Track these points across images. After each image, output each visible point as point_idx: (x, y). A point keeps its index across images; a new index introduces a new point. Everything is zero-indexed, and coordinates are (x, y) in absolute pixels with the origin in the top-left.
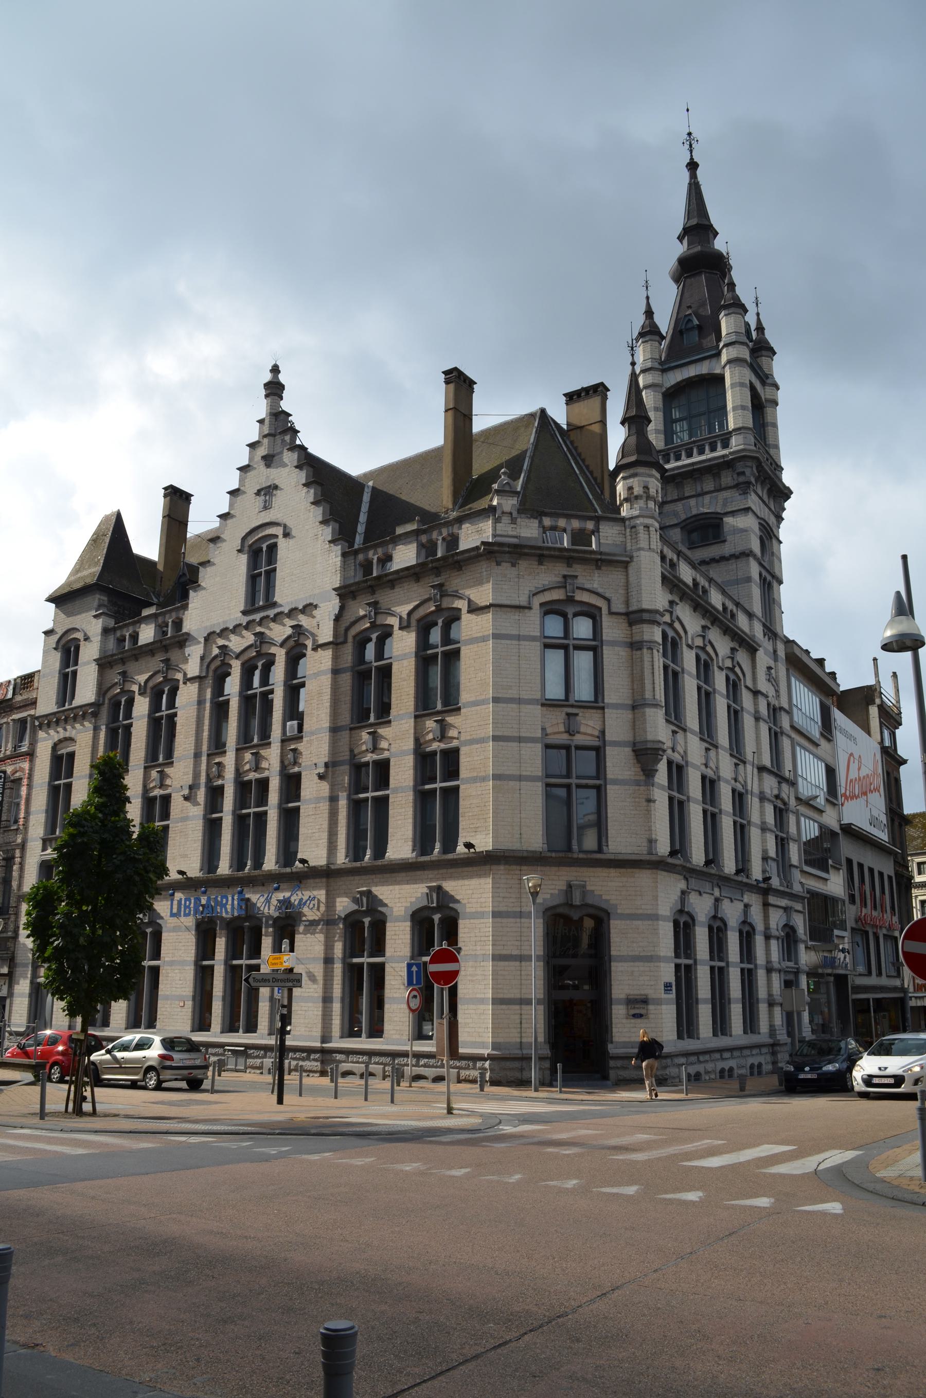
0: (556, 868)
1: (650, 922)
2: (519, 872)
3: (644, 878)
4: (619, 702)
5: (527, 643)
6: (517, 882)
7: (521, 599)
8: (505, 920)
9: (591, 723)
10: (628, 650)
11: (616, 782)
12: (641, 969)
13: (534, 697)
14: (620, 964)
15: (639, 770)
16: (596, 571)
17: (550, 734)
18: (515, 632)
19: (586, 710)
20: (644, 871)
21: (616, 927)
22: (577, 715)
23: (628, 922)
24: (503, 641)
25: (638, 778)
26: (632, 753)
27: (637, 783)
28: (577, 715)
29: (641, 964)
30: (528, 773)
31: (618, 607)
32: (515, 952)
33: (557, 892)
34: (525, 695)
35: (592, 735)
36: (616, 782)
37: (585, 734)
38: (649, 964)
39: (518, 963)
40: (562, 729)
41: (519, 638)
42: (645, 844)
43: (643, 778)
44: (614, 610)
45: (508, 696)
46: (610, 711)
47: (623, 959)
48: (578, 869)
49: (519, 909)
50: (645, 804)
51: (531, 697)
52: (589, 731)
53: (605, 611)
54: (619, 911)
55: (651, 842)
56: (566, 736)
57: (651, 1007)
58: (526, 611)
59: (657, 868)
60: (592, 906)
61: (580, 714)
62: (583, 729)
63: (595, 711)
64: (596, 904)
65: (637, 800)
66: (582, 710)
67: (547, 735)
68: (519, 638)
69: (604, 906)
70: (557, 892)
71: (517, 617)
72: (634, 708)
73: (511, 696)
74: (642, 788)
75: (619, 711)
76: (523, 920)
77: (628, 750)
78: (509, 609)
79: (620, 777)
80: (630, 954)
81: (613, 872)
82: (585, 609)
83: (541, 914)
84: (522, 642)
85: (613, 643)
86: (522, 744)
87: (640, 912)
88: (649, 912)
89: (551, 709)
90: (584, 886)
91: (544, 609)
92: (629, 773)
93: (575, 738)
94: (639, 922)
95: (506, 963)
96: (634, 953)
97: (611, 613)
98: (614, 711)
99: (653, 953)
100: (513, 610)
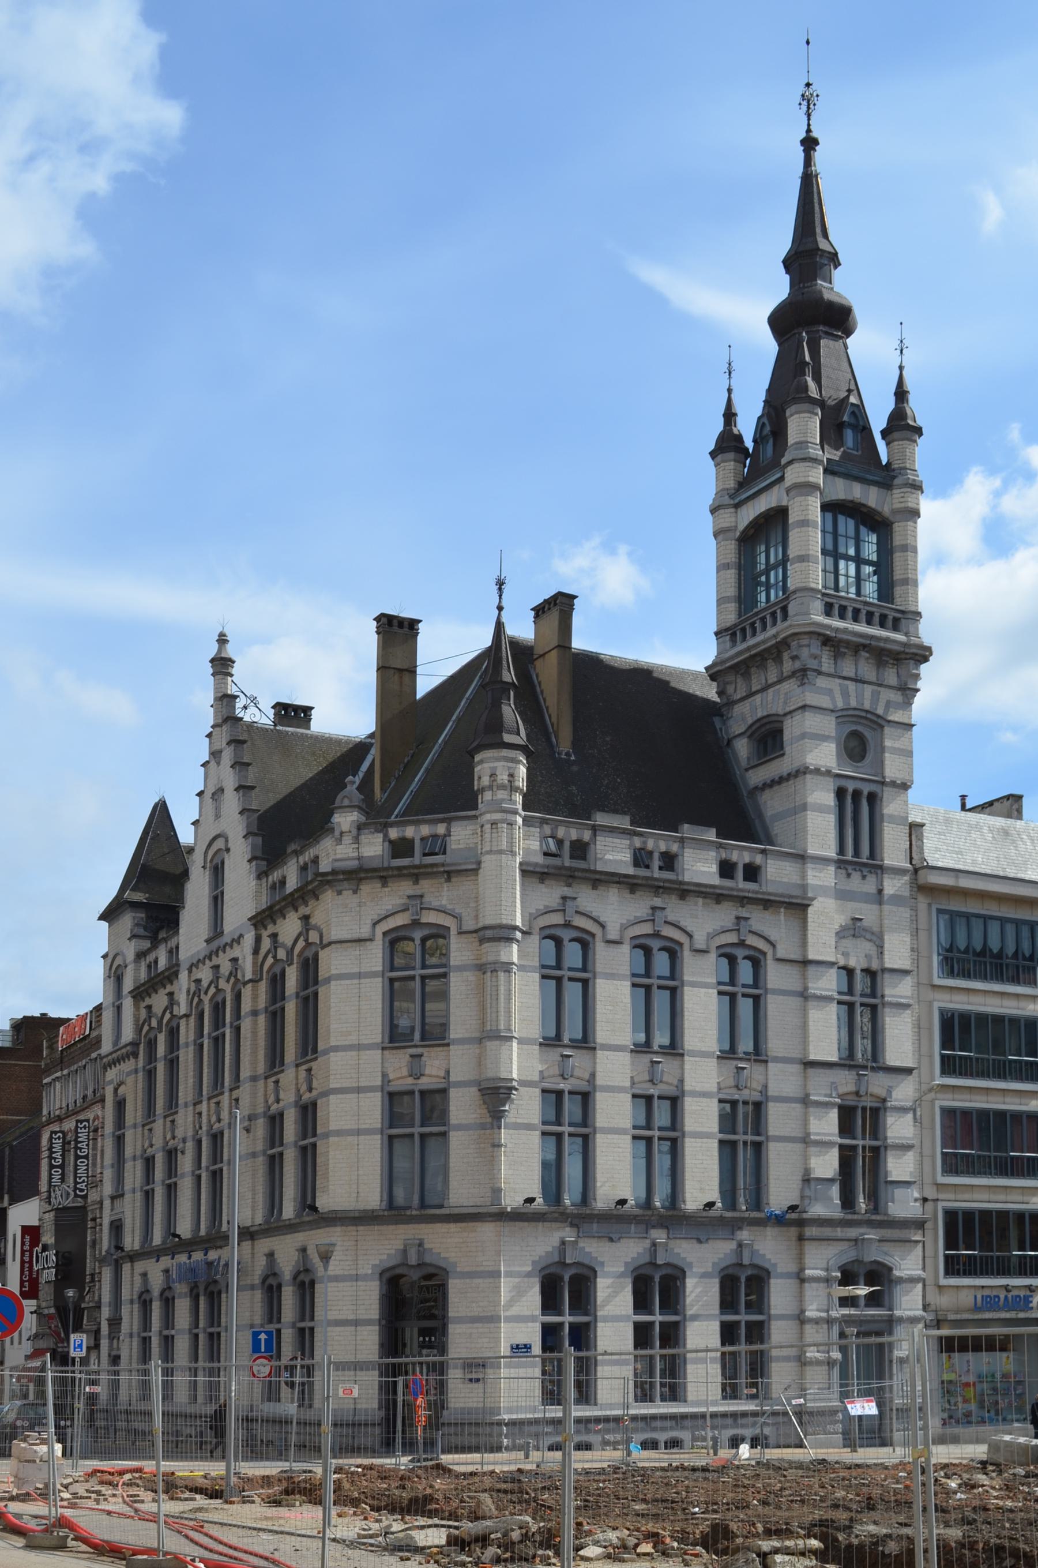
0: (393, 1227)
1: (491, 1280)
2: (354, 1233)
3: (487, 1230)
4: (467, 1035)
5: (368, 980)
6: (354, 1243)
7: (362, 931)
8: (341, 1284)
9: (436, 1062)
10: (477, 973)
11: (460, 1127)
12: (481, 1330)
13: (375, 1041)
14: (458, 1326)
15: (486, 1111)
16: (445, 885)
17: (393, 1080)
18: (356, 970)
19: (431, 1049)
20: (487, 1224)
21: (455, 1287)
22: (421, 1056)
23: (468, 1280)
24: (343, 982)
25: (483, 1121)
26: (478, 1093)
27: (483, 1127)
28: (421, 1056)
29: (480, 1325)
30: (367, 1126)
31: (469, 924)
32: (352, 1317)
33: (393, 1252)
34: (365, 1041)
35: (438, 1077)
36: (460, 1127)
37: (430, 1076)
38: (489, 1325)
39: (353, 1328)
40: (405, 1072)
41: (360, 976)
42: (489, 1194)
43: (489, 1120)
44: (465, 928)
45: (347, 1043)
46: (456, 1047)
47: (461, 1320)
48: (416, 1226)
49: (355, 1272)
50: (491, 1149)
51: (371, 1041)
52: (434, 1072)
53: (453, 931)
54: (458, 1269)
55: (497, 1192)
56: (410, 1081)
57: (489, 1371)
58: (368, 943)
59: (500, 1220)
60: (431, 1265)
61: (425, 1054)
62: (427, 1072)
63: (441, 1049)
64: (434, 1262)
65: (482, 1145)
66: (427, 1049)
67: (389, 1081)
68: (360, 976)
69: (443, 1265)
70: (393, 1252)
71: (358, 953)
72: (480, 1041)
73: (350, 1043)
74: (488, 1132)
75: (466, 1046)
76: (359, 1283)
77: (474, 1090)
78: (349, 944)
79: (464, 1122)
80: (469, 1314)
81: (453, 1227)
82: (434, 931)
83: (377, 1276)
84: (363, 981)
85: (461, 968)
86: (361, 1095)
87: (482, 1269)
88: (490, 1269)
89: (394, 1051)
90: (421, 1245)
91: (387, 939)
92: (474, 1116)
93: (420, 1081)
94: (480, 1281)
95: (342, 1328)
96: (472, 1314)
97: (460, 933)
98: (461, 1047)
99: (493, 1313)
100: (354, 944)
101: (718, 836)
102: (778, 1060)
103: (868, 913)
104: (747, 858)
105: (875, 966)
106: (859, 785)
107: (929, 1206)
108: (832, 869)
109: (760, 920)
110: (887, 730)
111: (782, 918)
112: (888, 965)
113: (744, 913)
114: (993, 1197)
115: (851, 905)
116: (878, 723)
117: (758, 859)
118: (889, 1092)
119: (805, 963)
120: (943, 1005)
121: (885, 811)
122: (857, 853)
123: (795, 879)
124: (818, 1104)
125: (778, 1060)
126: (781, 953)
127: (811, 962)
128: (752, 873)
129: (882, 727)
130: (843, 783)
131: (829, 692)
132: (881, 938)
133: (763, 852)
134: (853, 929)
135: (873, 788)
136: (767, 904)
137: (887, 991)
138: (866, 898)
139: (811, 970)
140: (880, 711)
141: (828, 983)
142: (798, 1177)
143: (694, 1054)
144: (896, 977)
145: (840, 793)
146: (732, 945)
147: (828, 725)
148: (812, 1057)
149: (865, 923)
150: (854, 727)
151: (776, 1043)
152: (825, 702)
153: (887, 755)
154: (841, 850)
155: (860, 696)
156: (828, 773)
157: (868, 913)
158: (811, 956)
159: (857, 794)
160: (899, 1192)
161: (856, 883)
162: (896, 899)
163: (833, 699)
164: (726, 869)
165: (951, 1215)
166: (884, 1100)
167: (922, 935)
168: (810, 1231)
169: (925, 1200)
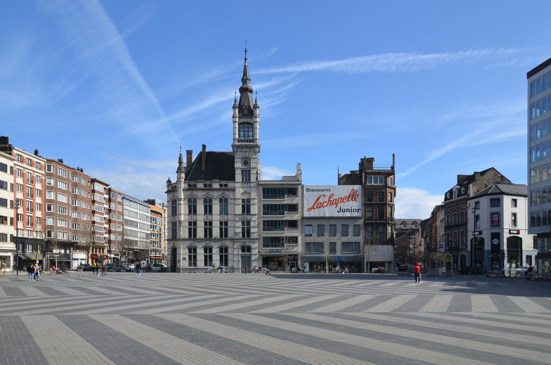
101: (219, 180)
102: (230, 214)
103: (248, 190)
104: (225, 183)
105: (249, 198)
106: (246, 169)
107: (260, 236)
108: (240, 183)
109: (226, 193)
110: (251, 159)
111: (231, 192)
112: (251, 198)
113: (224, 192)
114: (274, 234)
115: (244, 189)
116: (250, 159)
117: (227, 183)
118: (251, 219)
119: (235, 199)
120: (263, 203)
121: (251, 173)
122: (246, 180)
123: (234, 186)
124: (237, 221)
125: (230, 214)
126: (231, 197)
127: (236, 199)
128: (226, 185)
129: (250, 159)
130: (243, 169)
131: (240, 155)
132: (250, 193)
133: (227, 182)
134: (245, 193)
135: (249, 169)
136: (228, 190)
137: (251, 202)
138: (248, 187)
139: (236, 200)
140: (250, 156)
141: (240, 202)
142: (234, 232)
143: (214, 214)
144: (253, 200)
145: (242, 171)
146: (222, 197)
147: (240, 160)
148: (236, 214)
149: (247, 191)
150: (245, 160)
151: (230, 212)
152: (239, 156)
153: (251, 163)
154: (243, 179)
155: (246, 155)
156: (239, 168)
157: (248, 190)
158: (236, 198)
159: (246, 170)
160: (253, 234)
161: (246, 185)
162: (253, 187)
163: (240, 156)
164: (221, 185)
165: (264, 238)
166: (250, 220)
167: (260, 192)
168: (235, 241)
169: (259, 235)
